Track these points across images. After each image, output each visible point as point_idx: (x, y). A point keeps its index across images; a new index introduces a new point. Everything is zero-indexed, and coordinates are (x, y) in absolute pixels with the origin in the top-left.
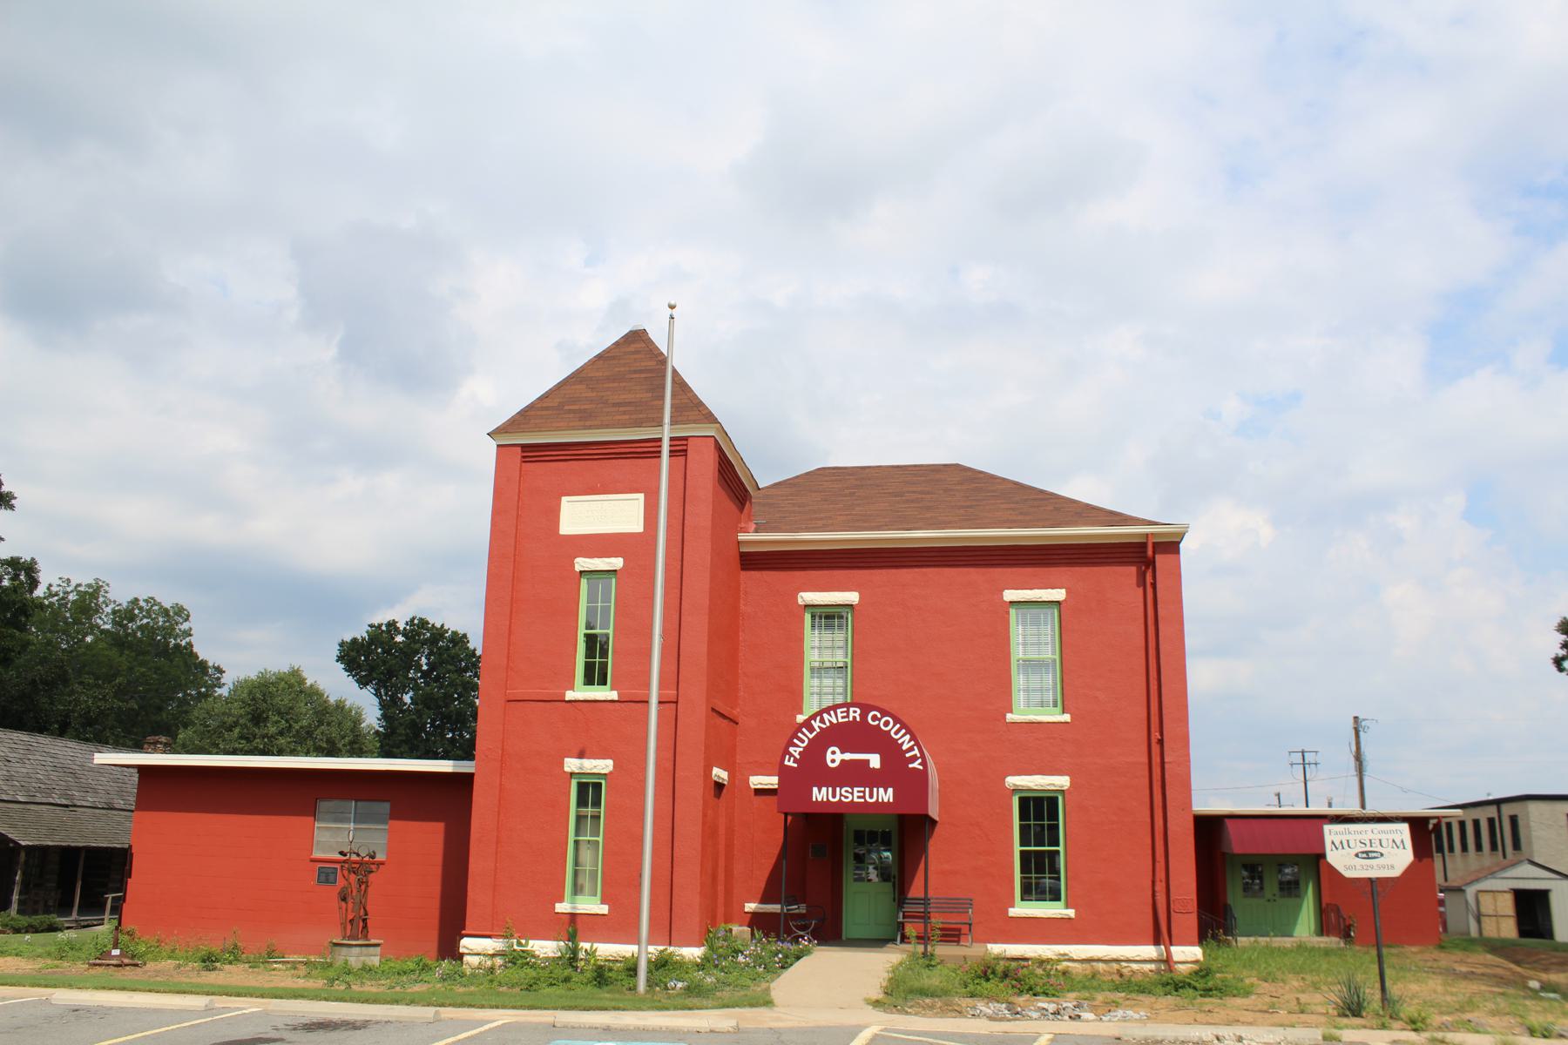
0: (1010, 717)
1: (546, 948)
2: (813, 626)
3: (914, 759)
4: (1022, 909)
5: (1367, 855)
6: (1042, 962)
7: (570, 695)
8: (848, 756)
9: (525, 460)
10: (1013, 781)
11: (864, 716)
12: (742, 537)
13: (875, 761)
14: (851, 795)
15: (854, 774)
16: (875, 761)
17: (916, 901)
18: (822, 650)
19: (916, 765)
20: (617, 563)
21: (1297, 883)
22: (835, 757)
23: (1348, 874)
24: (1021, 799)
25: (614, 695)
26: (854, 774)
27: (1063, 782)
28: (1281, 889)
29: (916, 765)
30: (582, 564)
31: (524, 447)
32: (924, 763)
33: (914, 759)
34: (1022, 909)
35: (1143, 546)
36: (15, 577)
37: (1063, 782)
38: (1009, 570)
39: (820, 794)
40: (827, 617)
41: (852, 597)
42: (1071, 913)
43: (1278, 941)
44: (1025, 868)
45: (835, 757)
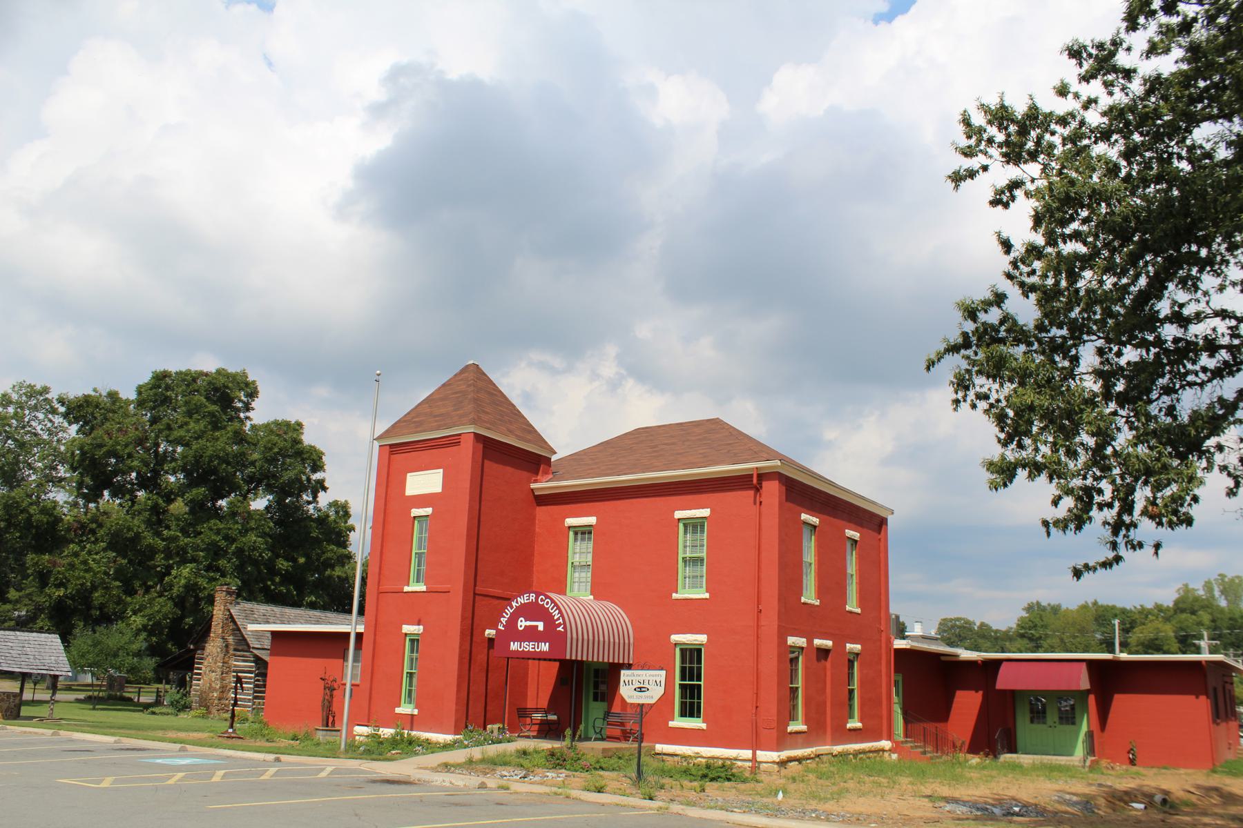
0: (675, 596)
1: (386, 732)
2: (576, 540)
3: (560, 625)
4: (679, 722)
5: (640, 689)
6: (685, 757)
7: (406, 589)
8: (528, 623)
9: (391, 453)
10: (675, 638)
11: (537, 598)
12: (533, 486)
13: (541, 626)
14: (528, 647)
15: (531, 634)
16: (541, 626)
17: (618, 715)
18: (580, 553)
19: (560, 629)
20: (429, 511)
21: (1044, 711)
22: (522, 624)
23: (629, 701)
24: (682, 650)
25: (424, 588)
26: (531, 634)
27: (702, 638)
28: (1061, 718)
29: (560, 629)
30: (415, 512)
31: (391, 446)
32: (565, 628)
33: (560, 625)
34: (679, 722)
35: (751, 476)
36: (337, 513)
37: (702, 638)
38: (704, 496)
39: (514, 646)
40: (583, 533)
41: (592, 520)
42: (704, 726)
43: (1062, 760)
44: (683, 696)
45: (522, 624)
